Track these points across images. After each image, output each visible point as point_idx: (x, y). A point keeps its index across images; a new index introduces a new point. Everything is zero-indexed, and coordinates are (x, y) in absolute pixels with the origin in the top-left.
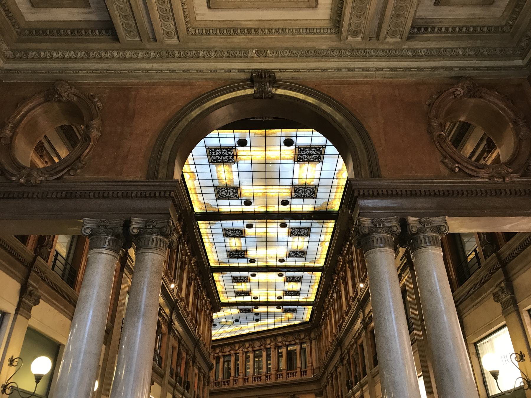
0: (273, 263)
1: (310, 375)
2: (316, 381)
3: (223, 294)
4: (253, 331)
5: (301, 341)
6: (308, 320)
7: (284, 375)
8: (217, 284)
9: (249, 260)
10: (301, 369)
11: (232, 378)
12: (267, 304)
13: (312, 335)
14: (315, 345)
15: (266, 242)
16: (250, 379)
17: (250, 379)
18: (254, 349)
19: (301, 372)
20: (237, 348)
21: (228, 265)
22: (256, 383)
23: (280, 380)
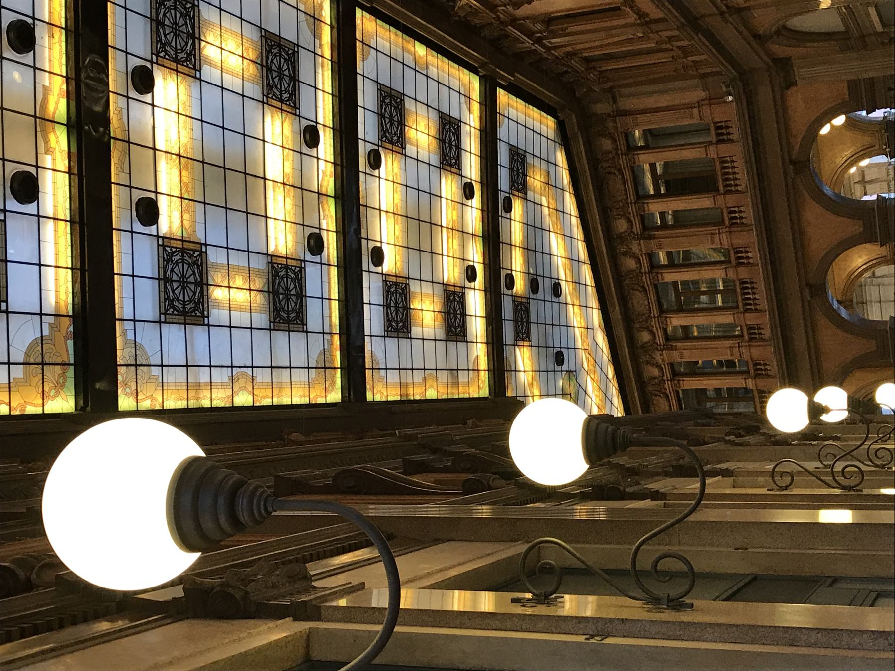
0: (323, 171)
1: (728, 110)
2: (744, 84)
3: (456, 384)
4: (596, 316)
5: (623, 147)
6: (551, 122)
7: (731, 200)
8: (416, 394)
9: (309, 257)
10: (710, 143)
11: (750, 384)
12: (493, 240)
13: (602, 108)
14: (633, 95)
15: (226, 178)
16: (751, 319)
17: (751, 319)
18: (655, 311)
19: (720, 142)
20: (656, 372)
21: (336, 338)
22: (762, 298)
23: (749, 215)
